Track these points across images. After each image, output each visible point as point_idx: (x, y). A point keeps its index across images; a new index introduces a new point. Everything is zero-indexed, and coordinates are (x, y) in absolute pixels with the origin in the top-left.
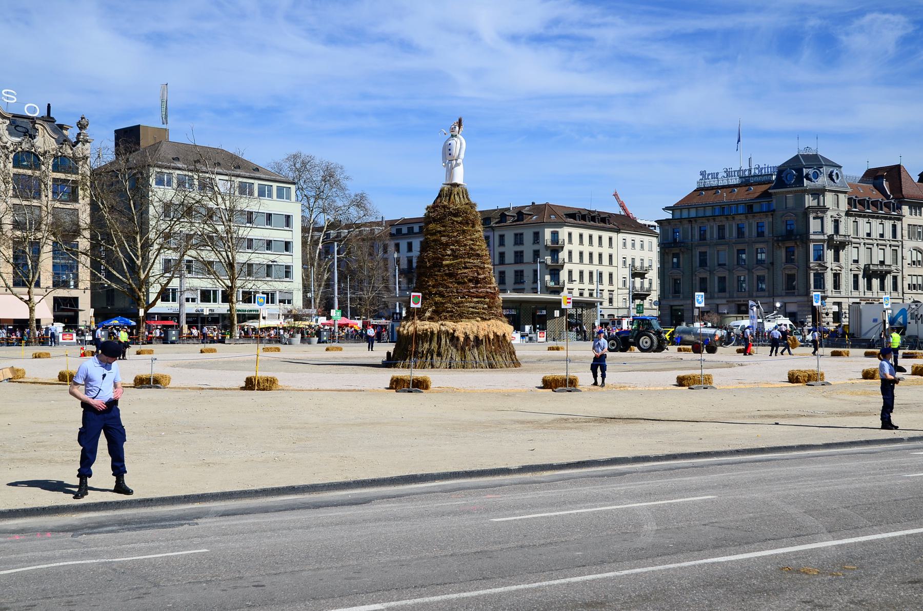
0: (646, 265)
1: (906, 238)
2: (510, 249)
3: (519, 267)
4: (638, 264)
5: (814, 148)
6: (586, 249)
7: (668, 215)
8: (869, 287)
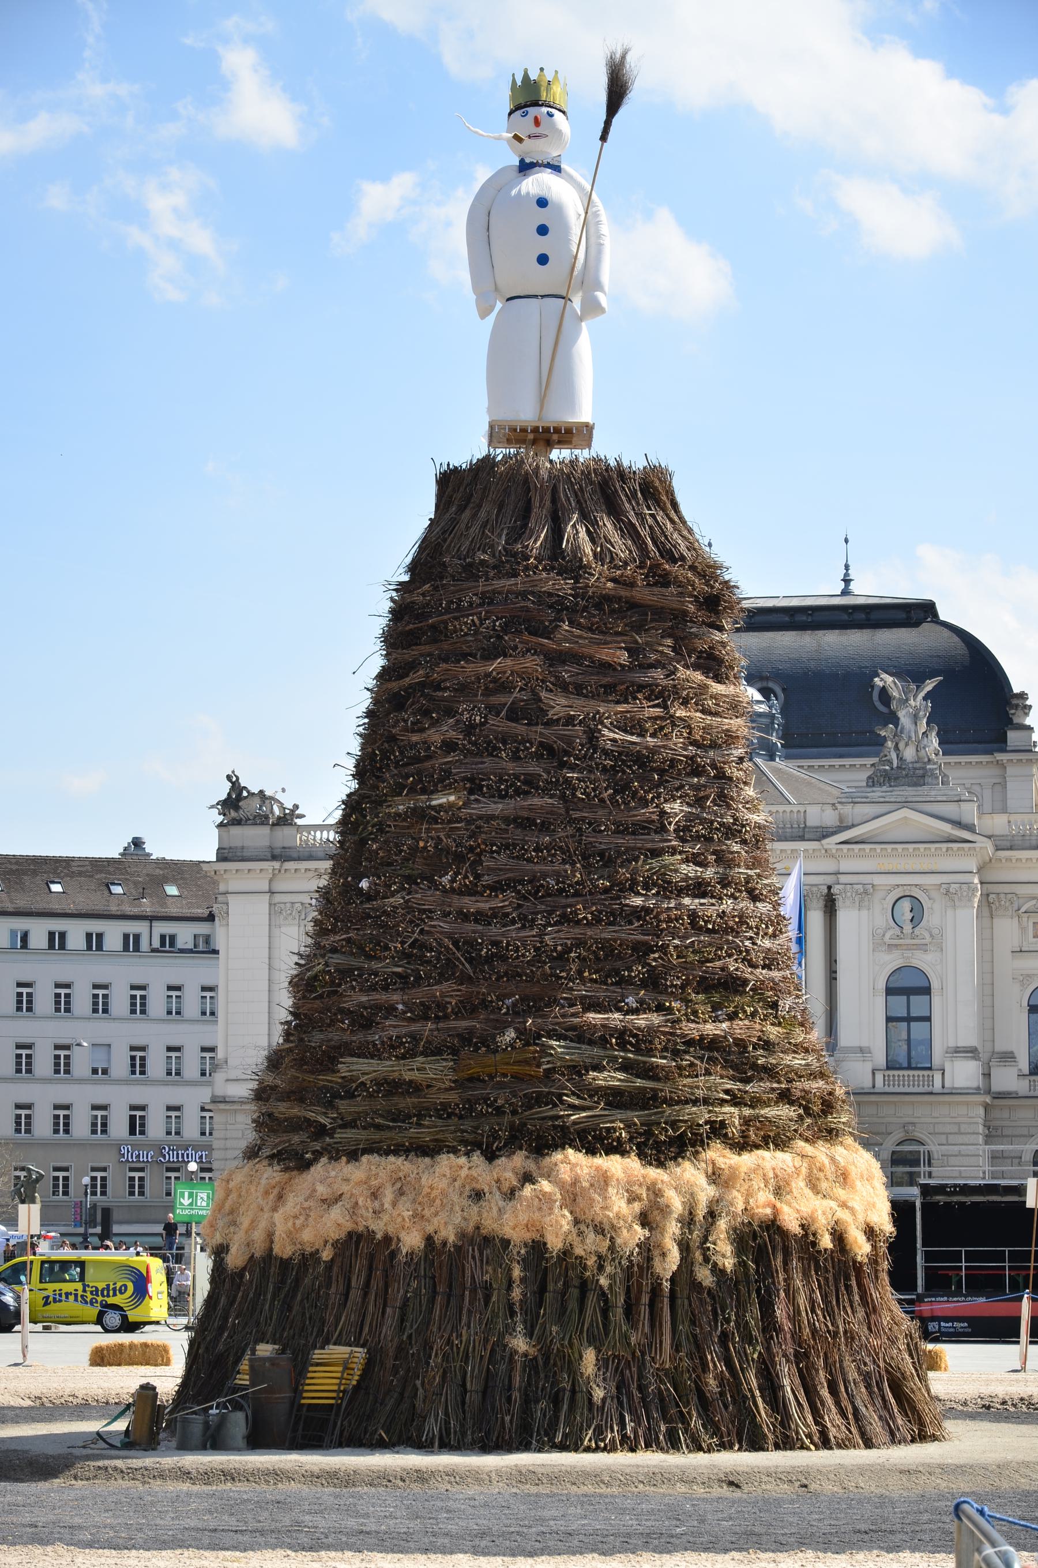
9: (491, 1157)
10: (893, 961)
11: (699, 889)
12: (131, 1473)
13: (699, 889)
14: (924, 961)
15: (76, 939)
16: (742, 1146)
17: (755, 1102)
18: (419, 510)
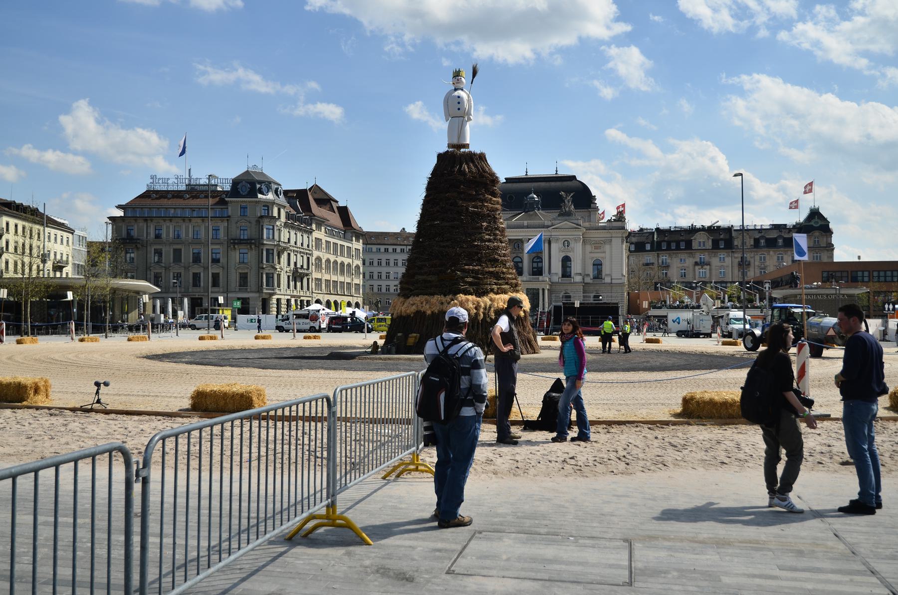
0: (65, 258)
4: (58, 257)
7: (120, 213)
8: (295, 288)
9: (445, 296)
10: (563, 255)
11: (489, 240)
12: (371, 359)
13: (489, 240)
14: (569, 254)
15: (390, 250)
16: (497, 293)
17: (500, 284)
18: (434, 161)
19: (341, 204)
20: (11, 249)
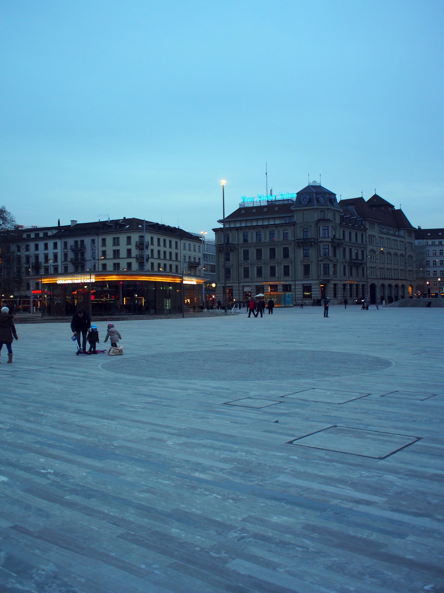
1: (368, 243)
2: (110, 248)
3: (116, 261)
4: (192, 260)
5: (318, 182)
6: (162, 249)
7: (221, 226)
19: (396, 208)
20: (156, 255)
